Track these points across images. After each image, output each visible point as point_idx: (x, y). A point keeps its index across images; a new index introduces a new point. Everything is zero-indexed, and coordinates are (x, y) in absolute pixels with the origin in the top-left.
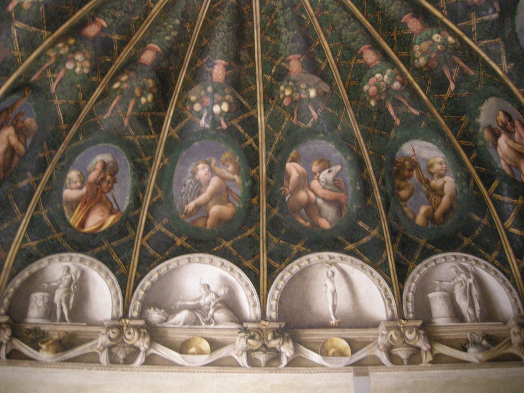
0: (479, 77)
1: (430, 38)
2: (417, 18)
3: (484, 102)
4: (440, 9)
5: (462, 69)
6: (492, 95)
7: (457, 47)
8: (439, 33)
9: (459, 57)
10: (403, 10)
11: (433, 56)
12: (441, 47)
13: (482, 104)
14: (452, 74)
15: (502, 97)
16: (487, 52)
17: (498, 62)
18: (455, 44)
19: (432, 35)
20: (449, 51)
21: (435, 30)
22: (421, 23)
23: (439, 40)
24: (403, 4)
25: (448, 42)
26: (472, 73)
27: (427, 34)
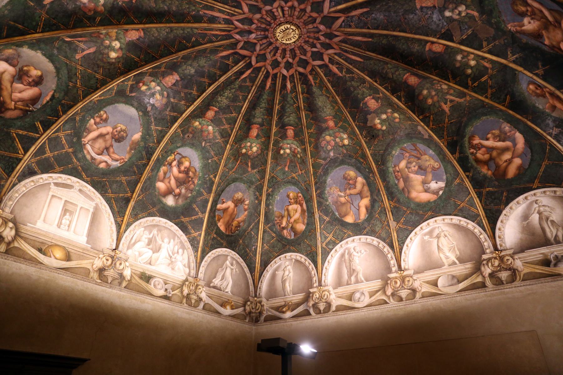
0: (75, 63)
1: (117, 39)
2: (138, 39)
3: (47, 58)
4: (147, 70)
5: (83, 50)
6: (58, 70)
7: (105, 56)
8: (121, 48)
9: (94, 53)
10: (148, 34)
11: (102, 36)
12: (107, 43)
13: (44, 55)
14: (79, 41)
15: (58, 80)
16: (109, 89)
17: (100, 96)
18: (109, 57)
19: (120, 42)
20: (102, 48)
21: (123, 46)
22: (133, 41)
23: (113, 45)
24: (153, 36)
25: (111, 50)
26: (78, 57)
27: (121, 39)
